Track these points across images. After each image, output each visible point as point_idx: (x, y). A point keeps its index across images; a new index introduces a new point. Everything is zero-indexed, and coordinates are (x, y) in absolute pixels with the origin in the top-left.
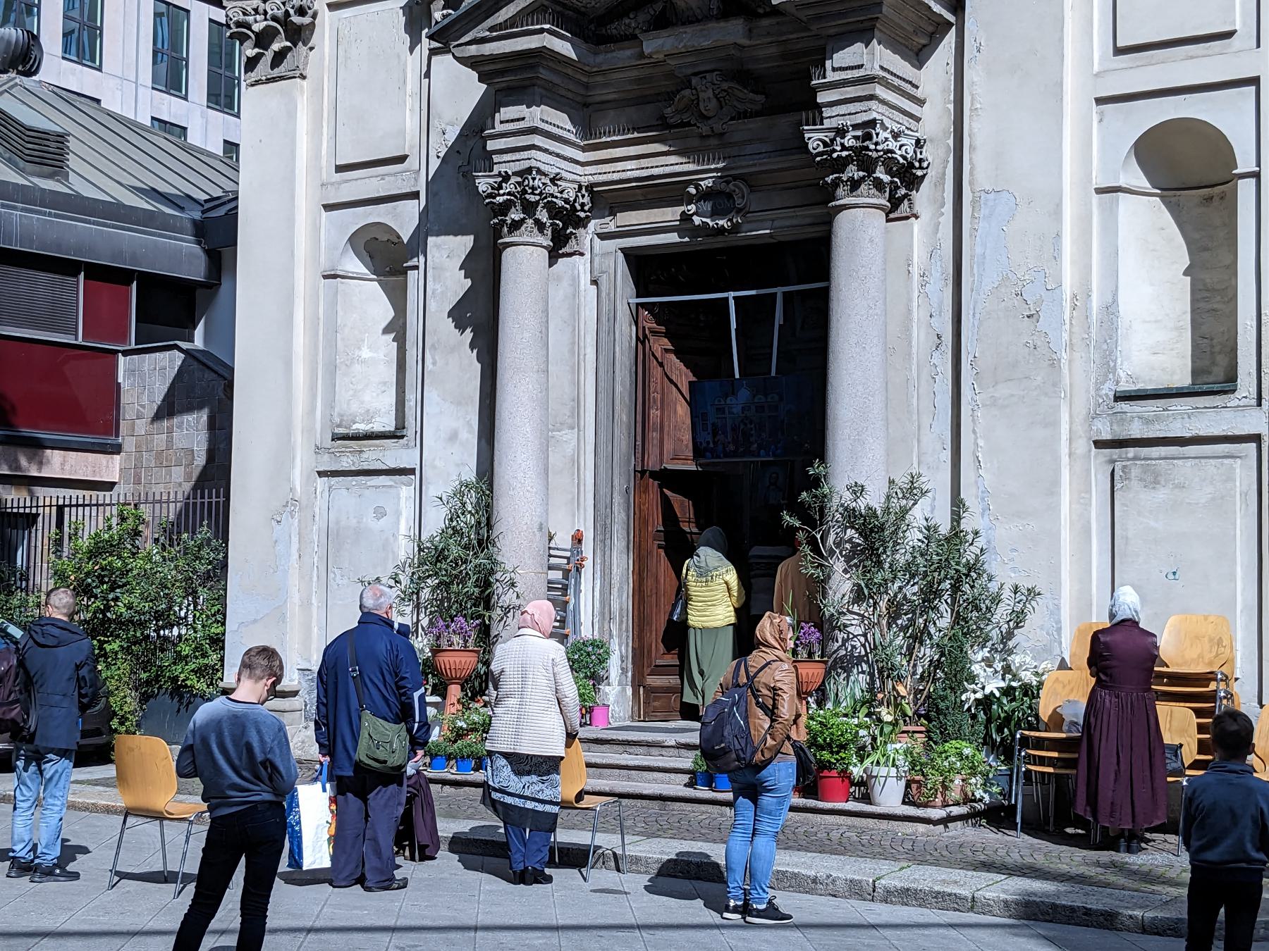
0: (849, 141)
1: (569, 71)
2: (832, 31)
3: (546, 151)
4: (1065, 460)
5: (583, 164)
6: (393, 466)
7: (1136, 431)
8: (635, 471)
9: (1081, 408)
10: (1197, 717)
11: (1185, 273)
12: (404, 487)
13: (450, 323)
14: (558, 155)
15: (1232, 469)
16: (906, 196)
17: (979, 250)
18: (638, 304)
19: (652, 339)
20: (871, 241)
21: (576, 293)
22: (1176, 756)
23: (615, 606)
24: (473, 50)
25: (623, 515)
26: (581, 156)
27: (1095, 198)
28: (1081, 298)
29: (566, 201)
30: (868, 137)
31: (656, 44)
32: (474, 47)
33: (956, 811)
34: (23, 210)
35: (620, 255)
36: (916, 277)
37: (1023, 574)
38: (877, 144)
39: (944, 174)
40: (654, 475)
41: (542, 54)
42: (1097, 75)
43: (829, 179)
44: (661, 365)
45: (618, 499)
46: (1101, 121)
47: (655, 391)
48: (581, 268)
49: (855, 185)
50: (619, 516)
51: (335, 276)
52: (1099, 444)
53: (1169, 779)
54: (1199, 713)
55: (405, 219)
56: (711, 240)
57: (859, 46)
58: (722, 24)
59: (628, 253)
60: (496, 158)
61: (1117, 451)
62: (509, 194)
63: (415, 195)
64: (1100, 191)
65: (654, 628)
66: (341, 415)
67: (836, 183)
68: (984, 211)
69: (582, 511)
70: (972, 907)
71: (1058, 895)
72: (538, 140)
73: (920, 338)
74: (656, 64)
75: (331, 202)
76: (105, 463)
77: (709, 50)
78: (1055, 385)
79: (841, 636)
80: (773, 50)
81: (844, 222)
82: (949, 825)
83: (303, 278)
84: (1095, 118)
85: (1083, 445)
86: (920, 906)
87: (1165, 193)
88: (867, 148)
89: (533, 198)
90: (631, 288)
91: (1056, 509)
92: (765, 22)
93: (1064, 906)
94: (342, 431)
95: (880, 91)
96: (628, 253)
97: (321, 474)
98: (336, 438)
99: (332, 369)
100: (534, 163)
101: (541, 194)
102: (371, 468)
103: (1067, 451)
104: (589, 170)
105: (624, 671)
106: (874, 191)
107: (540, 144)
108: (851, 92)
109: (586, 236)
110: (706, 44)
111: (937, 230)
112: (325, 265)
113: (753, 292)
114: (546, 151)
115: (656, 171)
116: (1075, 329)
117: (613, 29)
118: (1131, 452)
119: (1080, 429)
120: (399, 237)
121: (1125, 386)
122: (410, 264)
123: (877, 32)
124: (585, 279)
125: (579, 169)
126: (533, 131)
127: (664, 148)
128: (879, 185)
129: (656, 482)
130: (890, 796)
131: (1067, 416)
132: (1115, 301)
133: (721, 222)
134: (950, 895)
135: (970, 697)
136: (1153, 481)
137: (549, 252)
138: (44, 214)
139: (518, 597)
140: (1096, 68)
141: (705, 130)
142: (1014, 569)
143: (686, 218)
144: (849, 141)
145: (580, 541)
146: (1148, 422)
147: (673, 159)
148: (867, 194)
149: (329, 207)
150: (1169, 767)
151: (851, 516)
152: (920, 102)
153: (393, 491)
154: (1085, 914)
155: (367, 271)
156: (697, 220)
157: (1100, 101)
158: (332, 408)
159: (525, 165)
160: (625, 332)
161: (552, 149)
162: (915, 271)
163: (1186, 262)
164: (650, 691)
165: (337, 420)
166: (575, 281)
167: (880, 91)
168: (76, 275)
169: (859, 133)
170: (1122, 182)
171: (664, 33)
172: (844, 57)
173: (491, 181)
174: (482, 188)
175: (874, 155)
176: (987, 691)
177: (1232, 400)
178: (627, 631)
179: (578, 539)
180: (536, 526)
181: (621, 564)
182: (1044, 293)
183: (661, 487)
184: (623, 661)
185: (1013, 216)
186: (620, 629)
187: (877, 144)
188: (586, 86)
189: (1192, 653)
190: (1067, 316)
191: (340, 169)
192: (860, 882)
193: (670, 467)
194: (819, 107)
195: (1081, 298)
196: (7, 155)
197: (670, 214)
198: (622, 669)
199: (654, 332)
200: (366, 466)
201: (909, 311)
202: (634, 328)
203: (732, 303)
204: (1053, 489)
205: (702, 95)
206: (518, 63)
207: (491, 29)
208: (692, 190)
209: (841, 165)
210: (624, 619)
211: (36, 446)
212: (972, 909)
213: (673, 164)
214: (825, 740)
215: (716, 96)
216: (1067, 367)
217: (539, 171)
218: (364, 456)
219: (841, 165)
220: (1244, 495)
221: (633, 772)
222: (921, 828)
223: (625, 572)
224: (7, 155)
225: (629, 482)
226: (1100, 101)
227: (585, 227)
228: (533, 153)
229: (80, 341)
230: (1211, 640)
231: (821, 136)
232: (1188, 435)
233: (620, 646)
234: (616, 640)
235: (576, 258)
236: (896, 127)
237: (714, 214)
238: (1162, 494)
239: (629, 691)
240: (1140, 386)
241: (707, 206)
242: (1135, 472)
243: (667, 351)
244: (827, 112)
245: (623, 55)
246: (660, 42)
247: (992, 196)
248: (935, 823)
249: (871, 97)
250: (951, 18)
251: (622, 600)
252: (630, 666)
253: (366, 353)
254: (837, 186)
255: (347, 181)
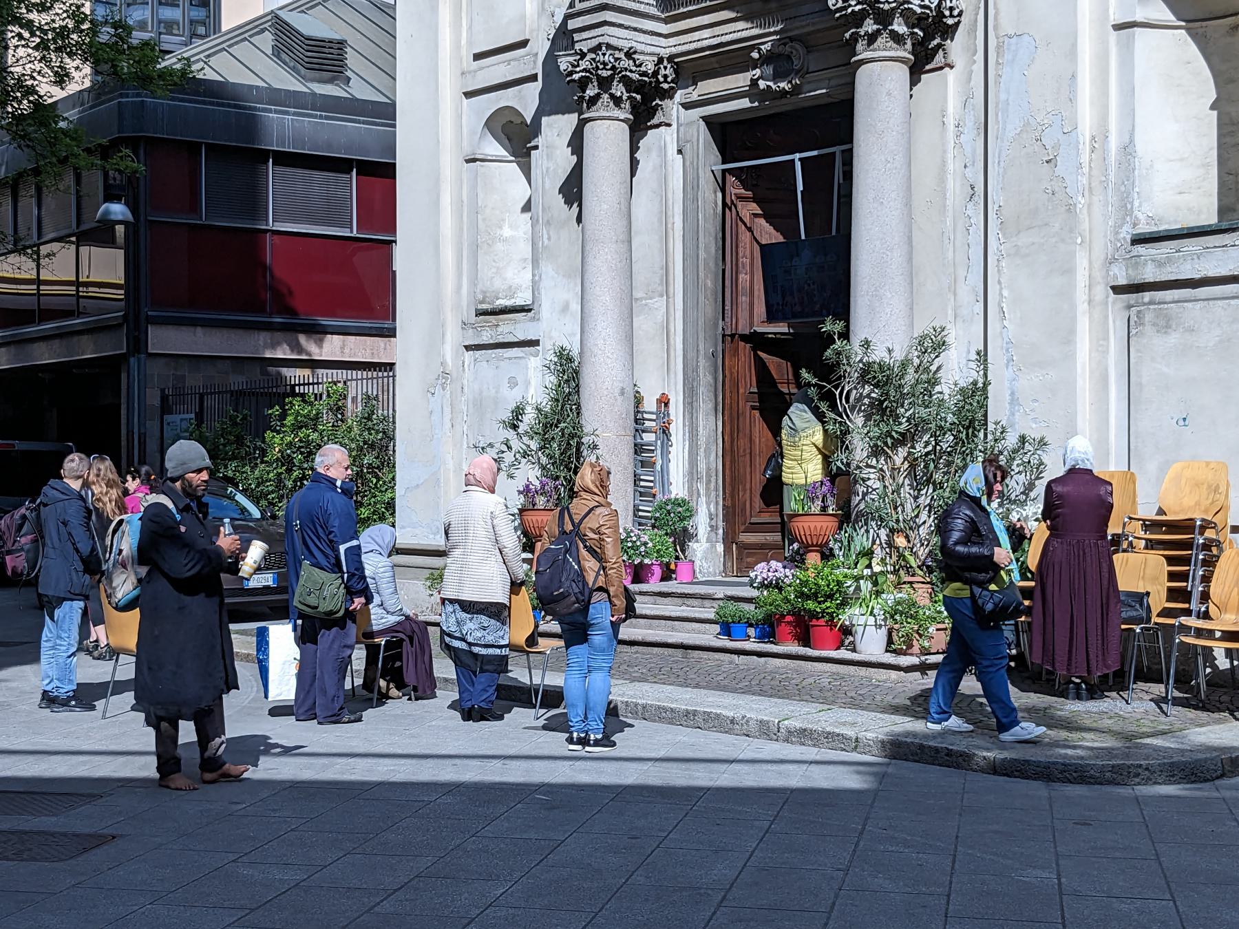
3: (620, 26)
4: (1082, 307)
8: (724, 336)
9: (1099, 253)
10: (1169, 565)
11: (1213, 107)
12: (532, 358)
14: (635, 29)
16: (939, 46)
17: (1003, 96)
18: (724, 171)
19: (740, 205)
20: (889, 94)
21: (664, 163)
22: (1141, 605)
23: (702, 466)
25: (710, 378)
27: (1113, 35)
28: (1099, 139)
29: (644, 74)
34: (295, 114)
35: (702, 123)
39: (976, 21)
40: (744, 338)
43: (847, 35)
44: (750, 229)
45: (702, 362)
48: (668, 139)
49: (872, 38)
50: (705, 379)
51: (474, 160)
52: (1117, 290)
53: (1123, 627)
54: (1171, 560)
55: (527, 100)
56: (778, 103)
59: (708, 120)
60: (576, 37)
62: (585, 70)
63: (534, 78)
64: (1118, 27)
65: (748, 486)
66: (484, 292)
67: (855, 38)
68: (1008, 56)
69: (672, 376)
70: (856, 747)
72: (609, 16)
73: (955, 189)
75: (470, 89)
76: (382, 345)
78: (1071, 231)
79: (861, 489)
83: (449, 163)
85: (1102, 291)
86: (814, 745)
87: (1191, 25)
89: (605, 74)
90: (715, 155)
91: (1071, 357)
93: (930, 747)
94: (485, 306)
96: (708, 120)
97: (468, 348)
98: (481, 313)
99: (475, 248)
100: (600, 40)
101: (613, 68)
102: (506, 340)
103: (1086, 297)
104: (672, 41)
105: (713, 528)
106: (891, 43)
107: (613, 20)
109: (672, 109)
111: (969, 80)
112: (468, 151)
113: (815, 153)
114: (620, 26)
116: (1094, 172)
118: (1147, 296)
119: (1098, 275)
121: (1144, 228)
122: (532, 144)
125: (663, 42)
127: (732, 15)
129: (748, 346)
130: (872, 643)
131: (1085, 263)
132: (1131, 141)
133: (782, 85)
136: (1165, 325)
138: (315, 116)
143: (754, 83)
145: (666, 405)
146: (1160, 264)
147: (741, 25)
149: (469, 95)
150: (1123, 615)
151: (866, 373)
153: (523, 361)
155: (507, 154)
156: (762, 84)
158: (475, 285)
159: (594, 43)
160: (710, 197)
161: (627, 23)
162: (951, 122)
163: (1213, 96)
164: (743, 547)
165: (480, 297)
168: (349, 172)
170: (1139, 18)
173: (571, 59)
174: (563, 67)
178: (716, 490)
179: (664, 402)
180: (617, 391)
181: (709, 425)
182: (1060, 136)
183: (754, 349)
186: (708, 489)
189: (1189, 501)
190: (1085, 158)
191: (478, 57)
192: (768, 722)
193: (760, 330)
195: (1099, 139)
196: (292, 64)
197: (740, 81)
198: (711, 526)
200: (501, 339)
201: (944, 163)
202: (720, 195)
203: (798, 165)
204: (1069, 338)
208: (755, 55)
211: (316, 331)
213: (742, 30)
216: (1085, 211)
217: (609, 46)
218: (500, 329)
219: (857, 19)
222: (894, 675)
223: (713, 434)
224: (292, 64)
225: (716, 346)
227: (671, 98)
229: (355, 234)
230: (1209, 486)
232: (1197, 276)
233: (708, 504)
234: (703, 499)
235: (662, 129)
237: (776, 77)
238: (1173, 338)
239: (720, 548)
241: (769, 70)
242: (1149, 317)
243: (756, 215)
251: (712, 460)
252: (721, 524)
253: (507, 232)
254: (857, 41)
255: (481, 69)
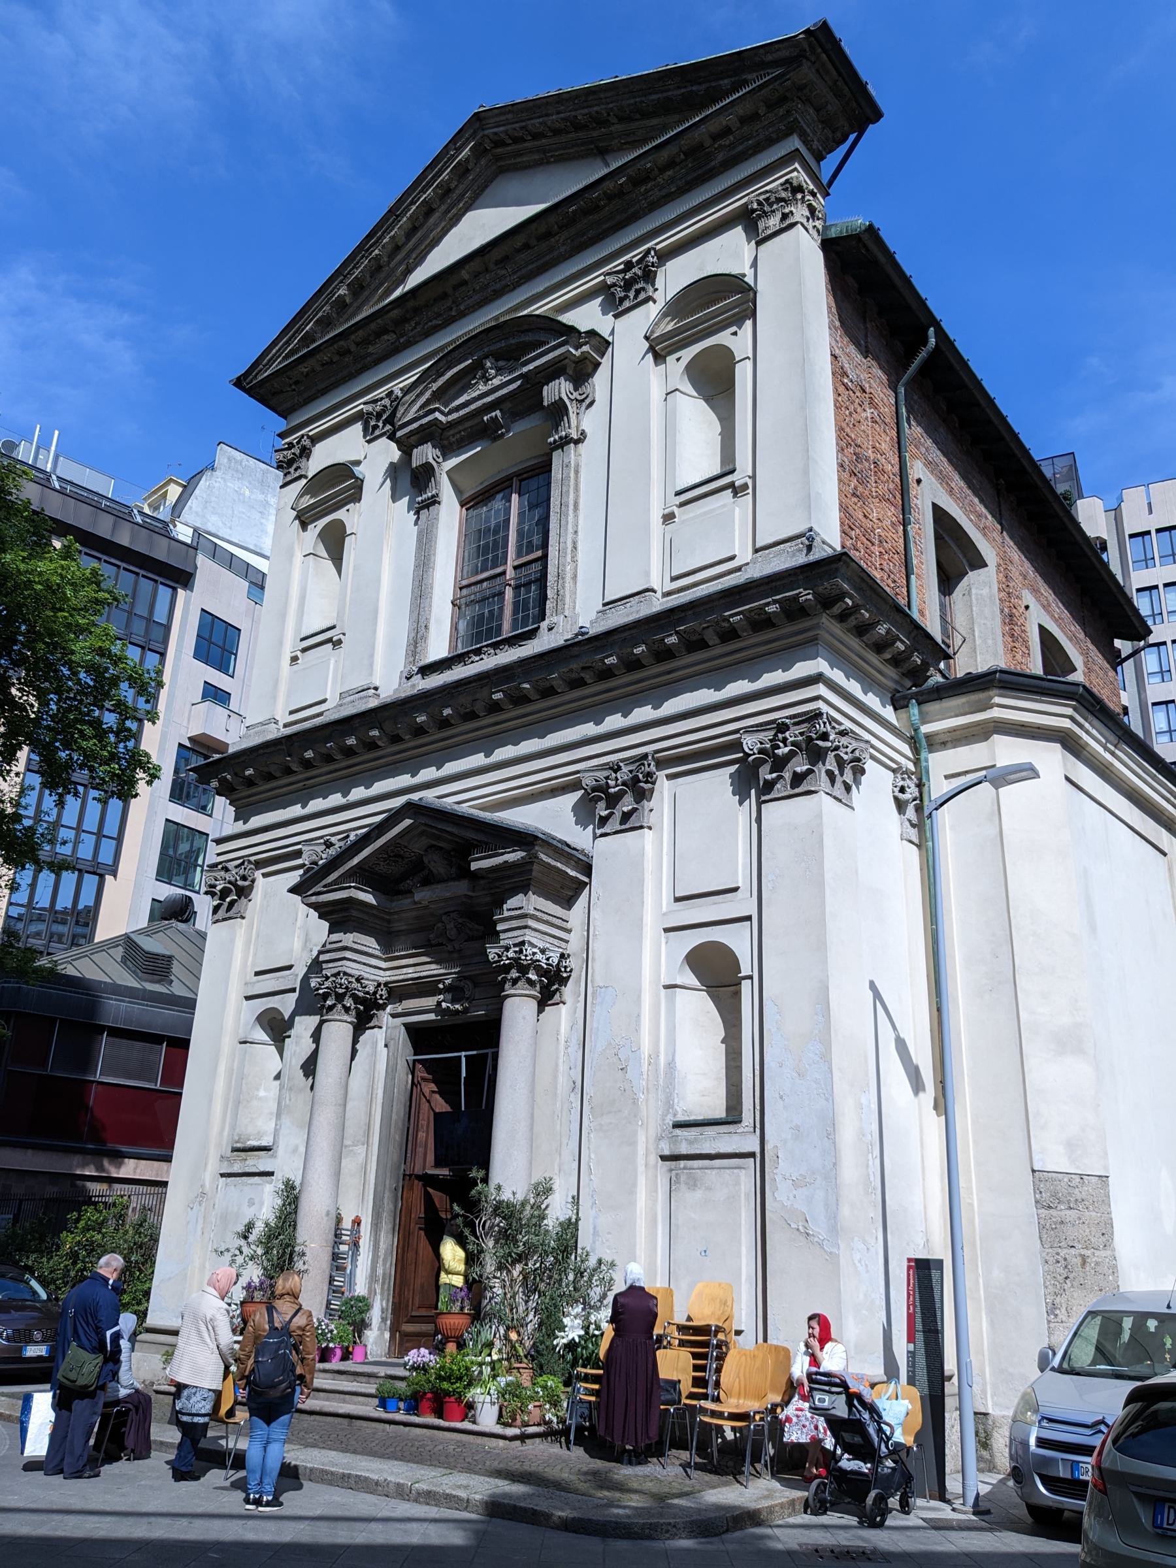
0: (511, 954)
1: (374, 912)
2: (507, 887)
3: (354, 961)
4: (641, 1168)
5: (384, 970)
6: (262, 1170)
7: (684, 1149)
8: (404, 1175)
9: (652, 1133)
10: (694, 1359)
11: (722, 1042)
12: (268, 1185)
13: (301, 1073)
14: (364, 964)
15: (739, 1176)
16: (557, 990)
17: (595, 1025)
18: (415, 1061)
19: (423, 1084)
20: (524, 1018)
21: (374, 1053)
22: (675, 1390)
23: (380, 1271)
24: (313, 899)
25: (391, 1206)
26: (383, 965)
27: (663, 991)
28: (654, 1056)
29: (368, 993)
30: (521, 952)
31: (422, 895)
32: (314, 897)
33: (531, 1430)
34: (129, 1002)
35: (403, 1028)
36: (562, 1042)
37: (614, 1251)
38: (526, 956)
39: (580, 975)
40: (418, 1177)
41: (350, 901)
42: (664, 914)
43: (500, 978)
44: (428, 1101)
45: (387, 1194)
46: (667, 943)
47: (423, 1119)
48: (379, 1037)
49: (515, 982)
50: (388, 1205)
51: (245, 1042)
52: (664, 1158)
53: (662, 1407)
54: (695, 1356)
55: (286, 1005)
56: (453, 1018)
57: (521, 896)
58: (457, 883)
59: (407, 1026)
60: (324, 966)
61: (674, 1163)
62: (327, 988)
63: (293, 990)
64: (667, 987)
65: (411, 1288)
66: (240, 1135)
67: (504, 980)
68: (599, 1000)
69: (365, 1203)
70: (467, 1507)
71: (524, 1497)
72: (348, 954)
73: (563, 1083)
74: (426, 907)
75: (249, 994)
76: (166, 1168)
77: (451, 899)
78: (635, 1116)
79: (489, 1295)
80: (488, 899)
81: (509, 1005)
82: (527, 1441)
83: (228, 1042)
84: (663, 941)
85: (654, 1159)
86: (436, 1505)
87: (710, 989)
88: (520, 959)
89: (341, 991)
90: (409, 1049)
91: (633, 1204)
92: (482, 882)
93: (521, 1507)
94: (238, 1145)
95: (531, 923)
96: (407, 1026)
97: (222, 1175)
98: (235, 1150)
99: (238, 1103)
100: (340, 969)
101: (347, 988)
102: (250, 1171)
103: (643, 1162)
104: (388, 973)
105: (384, 1320)
106: (527, 986)
107: (350, 957)
108: (514, 924)
109: (384, 1017)
110: (448, 895)
111: (575, 1012)
112: (242, 1037)
113: (474, 1053)
114: (354, 961)
115: (422, 974)
116: (650, 1078)
117: (402, 887)
118: (682, 1163)
119: (652, 1148)
120: (281, 1014)
121: (681, 1118)
122: (287, 1034)
123: (531, 887)
124: (381, 1043)
125: (382, 973)
126: (345, 948)
127: (429, 960)
128: (531, 983)
129: (421, 1183)
130: (487, 1418)
131: (644, 1139)
132: (673, 1060)
133: (457, 1006)
134: (454, 1496)
135: (561, 1341)
136: (693, 1184)
137: (354, 1028)
138: (143, 1005)
139: (304, 1263)
140: (664, 910)
141: (450, 948)
142: (609, 1248)
143: (439, 1004)
144: (511, 954)
145: (359, 1224)
146: (690, 1143)
147: (433, 966)
148: (522, 988)
149: (248, 998)
150: (662, 1398)
151: (500, 1209)
152: (569, 931)
153: (260, 1187)
154: (533, 1514)
155: (268, 1039)
156: (444, 1005)
157: (666, 930)
158: (234, 1129)
159: (336, 970)
160: (404, 1078)
161: (359, 960)
162: (562, 1039)
163: (723, 1034)
164: (405, 1336)
165: (237, 1138)
166: (375, 1044)
167: (531, 923)
168: (161, 1044)
169: (517, 949)
170: (679, 982)
171: (425, 888)
172: (512, 902)
173: (319, 980)
174: (313, 985)
175: (525, 963)
176: (570, 1337)
177: (740, 1128)
178: (389, 1289)
179: (357, 1222)
180: (324, 1213)
181: (387, 1241)
182: (630, 1053)
183: (425, 1186)
184: (383, 1312)
185: (614, 1003)
186: (382, 1288)
187: (526, 956)
188: (389, 922)
189: (707, 1311)
190: (645, 1068)
191: (257, 974)
192: (403, 1485)
193: (430, 1172)
194: (497, 933)
195: (654, 1056)
196: (133, 969)
197: (430, 1002)
198: (382, 1318)
199: (424, 1079)
200: (248, 1170)
201: (557, 1065)
202: (410, 1077)
203: (464, 1060)
204: (632, 1190)
205: (448, 927)
206: (340, 907)
207: (325, 886)
208: (441, 986)
209: (507, 969)
210: (387, 1281)
211: (118, 1157)
212: (466, 1509)
213: (434, 969)
214: (446, 1373)
215: (455, 927)
216: (644, 1103)
217: (345, 974)
218: (247, 1162)
219: (507, 969)
220: (747, 1195)
221: (347, 1396)
222: (501, 1443)
223: (390, 1247)
224: (133, 969)
225: (398, 1182)
226: (666, 930)
227: (384, 1009)
228: (344, 962)
229: (158, 1087)
230: (721, 1301)
231: (497, 950)
232: (713, 1152)
233: (382, 1301)
234: (378, 1297)
235: (376, 1030)
236: (541, 945)
237: (453, 1002)
238: (699, 1194)
239: (387, 1335)
240: (692, 1118)
241: (449, 996)
242: (683, 1178)
243: (433, 1092)
244: (502, 936)
245: (405, 902)
246: (424, 893)
247: (603, 989)
248: (512, 1438)
249: (526, 927)
250: (586, 880)
251: (386, 1268)
252: (389, 1316)
253: (262, 1093)
254: (505, 982)
255: (258, 982)
